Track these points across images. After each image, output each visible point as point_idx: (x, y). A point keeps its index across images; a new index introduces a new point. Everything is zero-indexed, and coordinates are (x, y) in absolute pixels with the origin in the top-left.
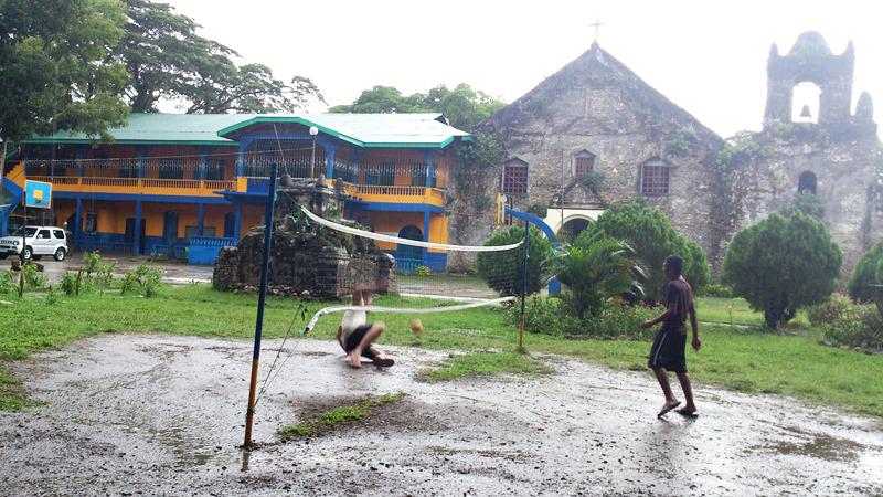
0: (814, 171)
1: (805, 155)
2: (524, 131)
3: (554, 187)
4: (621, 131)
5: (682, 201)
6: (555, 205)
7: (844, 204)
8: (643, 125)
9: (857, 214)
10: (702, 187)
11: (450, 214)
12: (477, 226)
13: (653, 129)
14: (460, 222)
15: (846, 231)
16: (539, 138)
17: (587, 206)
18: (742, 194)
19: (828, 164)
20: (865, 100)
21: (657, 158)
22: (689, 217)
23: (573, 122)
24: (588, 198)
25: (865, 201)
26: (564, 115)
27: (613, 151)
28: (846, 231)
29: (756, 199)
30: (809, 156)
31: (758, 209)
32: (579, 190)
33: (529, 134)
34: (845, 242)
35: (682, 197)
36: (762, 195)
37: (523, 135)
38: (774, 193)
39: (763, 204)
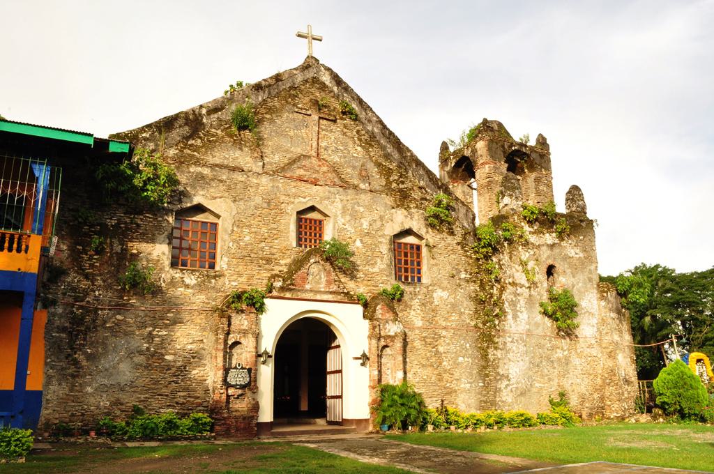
1: (548, 245)
2: (211, 160)
3: (269, 261)
4: (362, 186)
5: (445, 294)
6: (275, 293)
8: (389, 183)
10: (463, 276)
11: (54, 303)
12: (117, 330)
13: (401, 191)
14: (77, 321)
16: (240, 177)
17: (325, 297)
19: (566, 258)
20: (574, 194)
21: (408, 232)
22: (455, 317)
23: (293, 161)
24: (329, 283)
25: (595, 302)
26: (278, 149)
27: (355, 216)
29: (516, 294)
30: (552, 246)
31: (518, 309)
32: (314, 269)
33: (221, 166)
35: (444, 289)
36: (519, 290)
37: (213, 166)
38: (530, 287)
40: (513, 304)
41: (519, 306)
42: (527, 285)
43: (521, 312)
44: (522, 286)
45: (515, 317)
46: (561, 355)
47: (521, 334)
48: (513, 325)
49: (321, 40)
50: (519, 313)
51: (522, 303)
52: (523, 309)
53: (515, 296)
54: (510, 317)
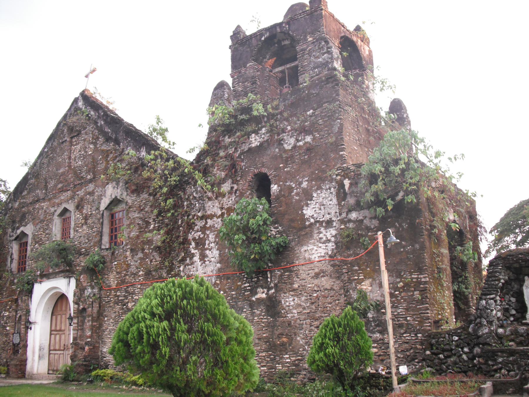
0: (264, 170)
7: (308, 212)
9: (329, 223)
15: (315, 257)
18: (190, 226)
25: (335, 201)
28: (315, 257)
31: (206, 246)
34: (317, 276)
36: (210, 222)
39: (212, 237)
40: (200, 243)
41: (207, 242)
42: (219, 213)
43: (210, 250)
44: (211, 217)
45: (203, 257)
46: (264, 296)
47: (209, 276)
48: (199, 267)
49: (94, 71)
50: (207, 252)
51: (212, 237)
52: (213, 245)
53: (204, 233)
54: (196, 259)
